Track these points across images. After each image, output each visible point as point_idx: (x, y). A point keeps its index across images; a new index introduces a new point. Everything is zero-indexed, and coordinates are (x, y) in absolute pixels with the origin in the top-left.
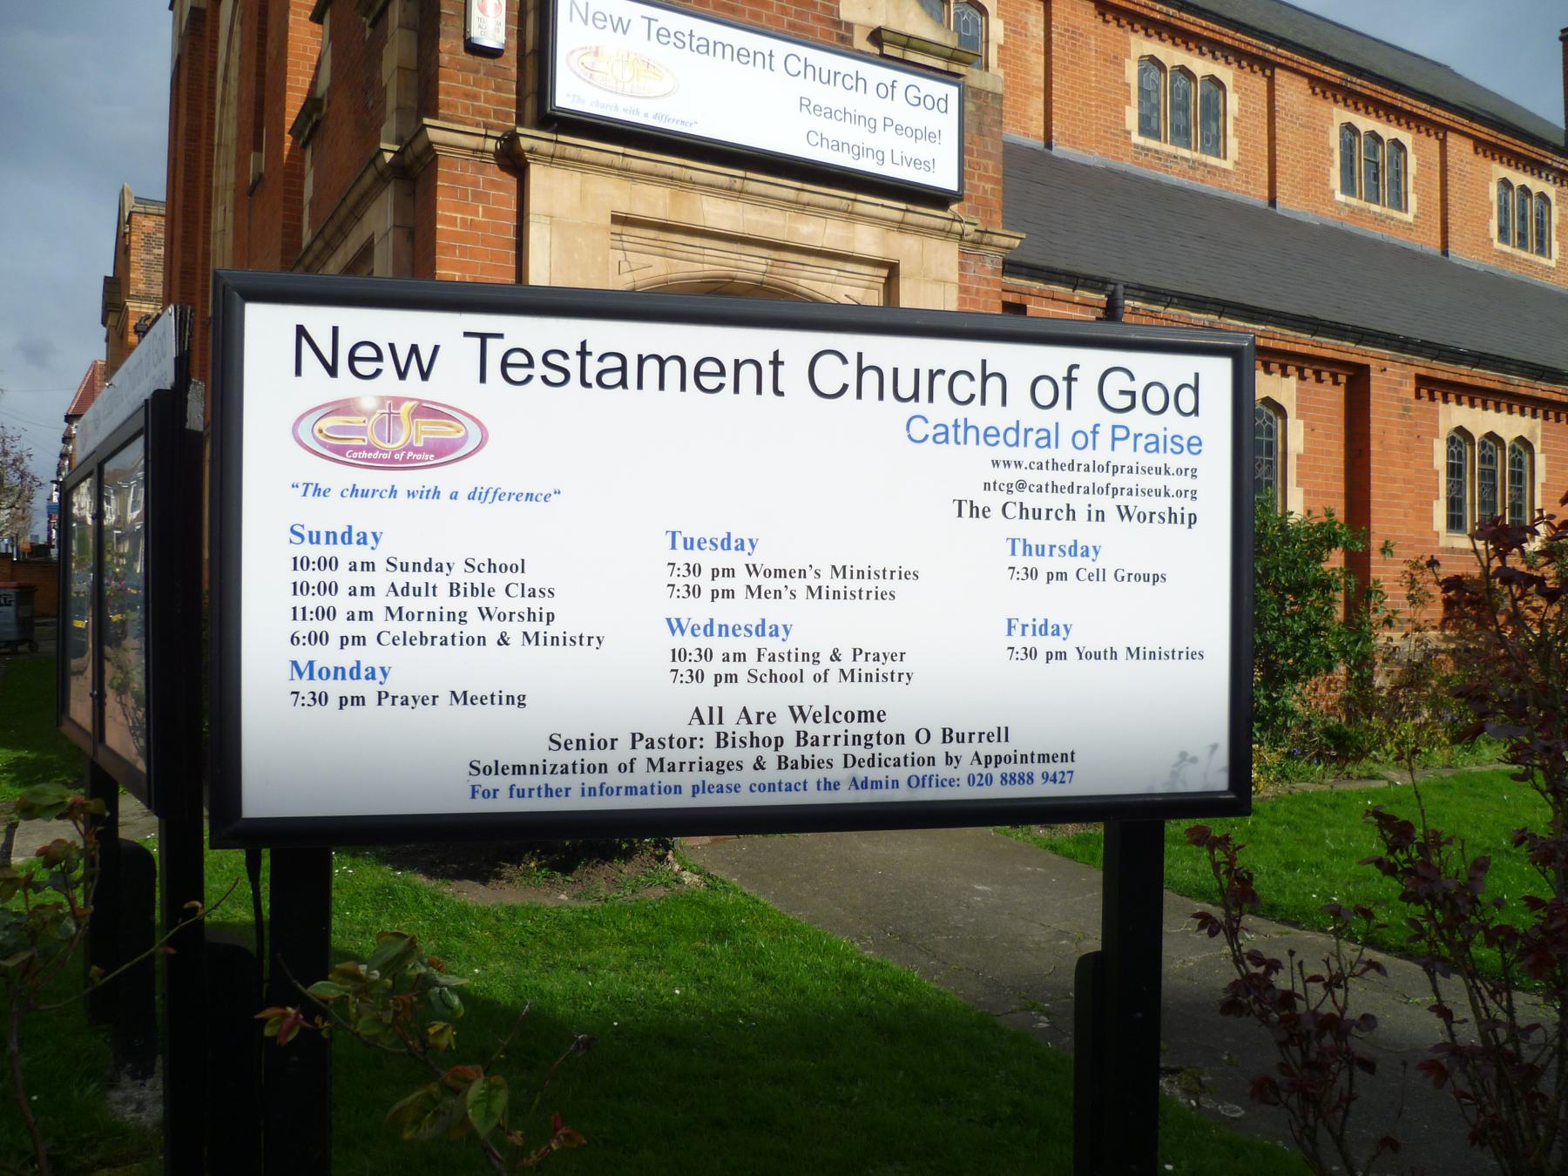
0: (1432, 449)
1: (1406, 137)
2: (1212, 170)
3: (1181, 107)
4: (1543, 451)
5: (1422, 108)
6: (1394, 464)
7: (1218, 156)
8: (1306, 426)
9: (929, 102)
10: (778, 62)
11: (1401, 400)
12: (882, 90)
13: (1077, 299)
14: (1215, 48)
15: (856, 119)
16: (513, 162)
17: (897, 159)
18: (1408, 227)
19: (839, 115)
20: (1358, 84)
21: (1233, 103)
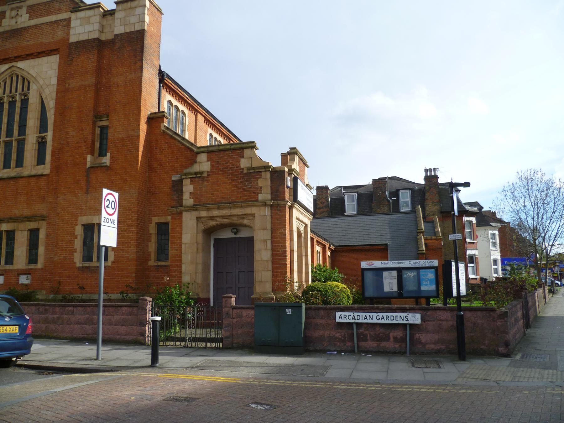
16: (291, 208)
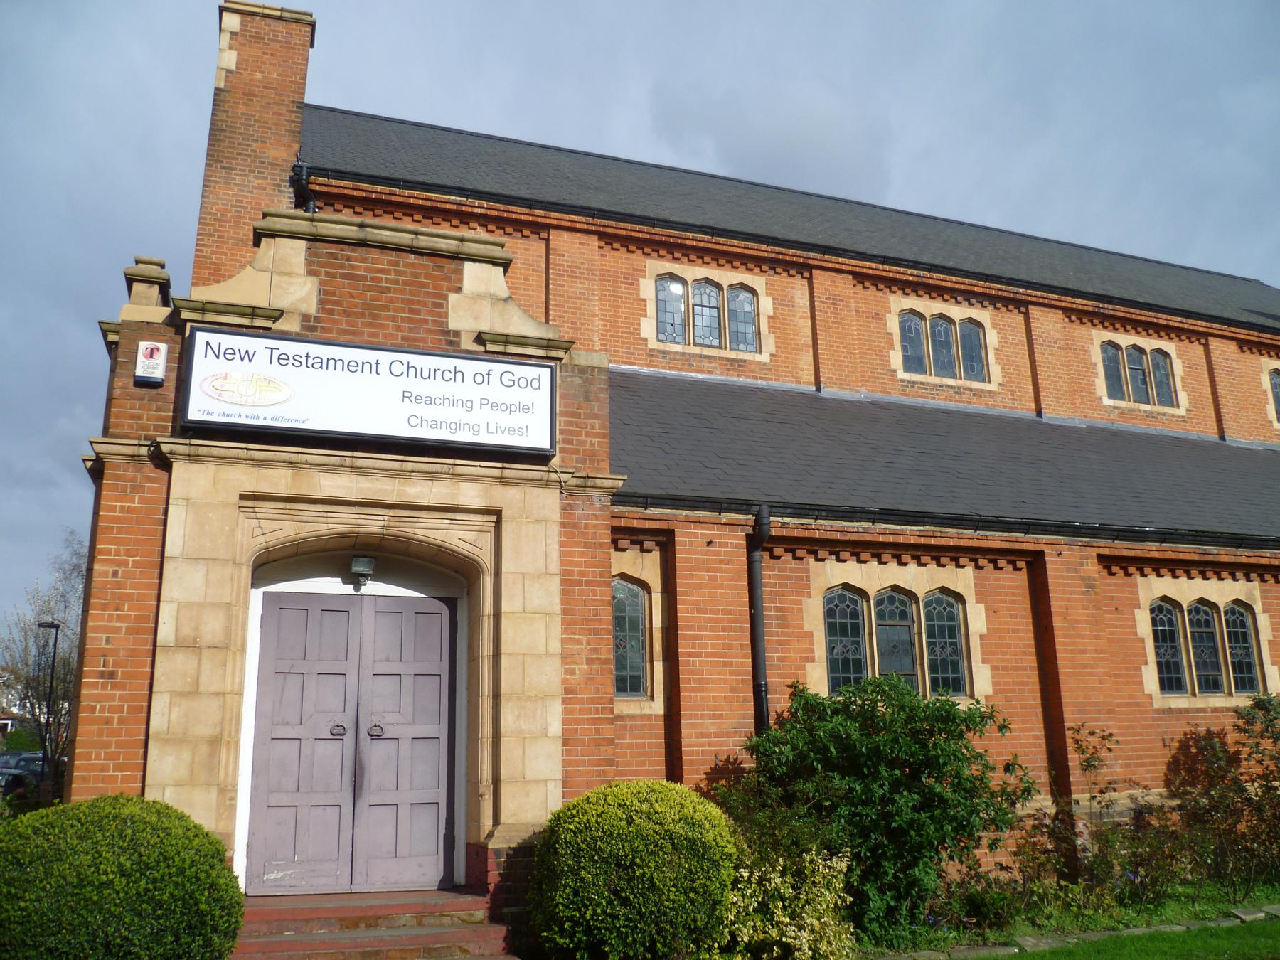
0: (1134, 620)
1: (1169, 346)
2: (978, 393)
4: (1265, 611)
5: (1178, 321)
6: (1082, 637)
7: (984, 381)
8: (987, 609)
9: (523, 383)
10: (383, 368)
11: (1083, 579)
12: (479, 378)
13: (724, 521)
14: (969, 297)
15: (454, 403)
17: (492, 429)
18: (1182, 419)
19: (438, 401)
20: (1111, 309)
21: (992, 338)
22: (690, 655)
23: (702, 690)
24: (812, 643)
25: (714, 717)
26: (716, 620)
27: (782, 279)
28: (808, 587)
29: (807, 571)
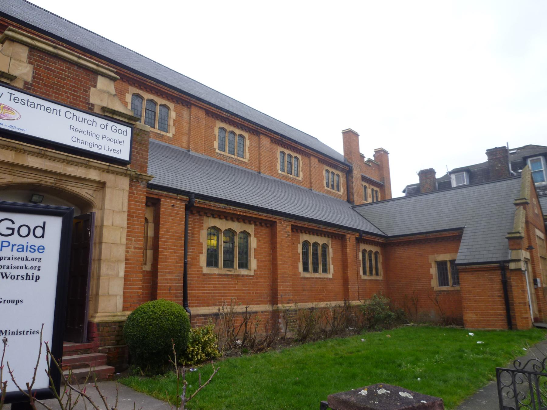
3: (232, 143)
7: (243, 158)
9: (120, 132)
10: (62, 113)
11: (286, 232)
12: (103, 126)
13: (179, 198)
15: (92, 134)
17: (107, 149)
18: (300, 182)
19: (85, 133)
21: (248, 143)
22: (163, 248)
23: (166, 262)
24: (202, 247)
25: (169, 272)
26: (173, 236)
27: (180, 107)
28: (202, 226)
29: (203, 220)
